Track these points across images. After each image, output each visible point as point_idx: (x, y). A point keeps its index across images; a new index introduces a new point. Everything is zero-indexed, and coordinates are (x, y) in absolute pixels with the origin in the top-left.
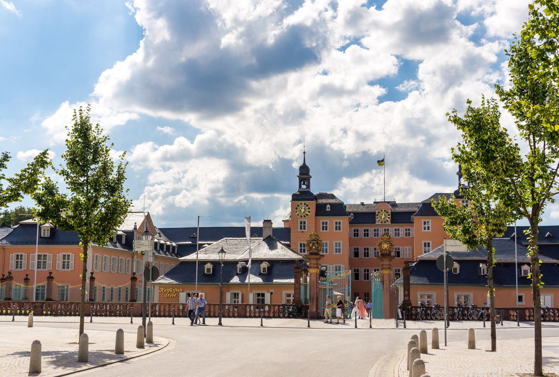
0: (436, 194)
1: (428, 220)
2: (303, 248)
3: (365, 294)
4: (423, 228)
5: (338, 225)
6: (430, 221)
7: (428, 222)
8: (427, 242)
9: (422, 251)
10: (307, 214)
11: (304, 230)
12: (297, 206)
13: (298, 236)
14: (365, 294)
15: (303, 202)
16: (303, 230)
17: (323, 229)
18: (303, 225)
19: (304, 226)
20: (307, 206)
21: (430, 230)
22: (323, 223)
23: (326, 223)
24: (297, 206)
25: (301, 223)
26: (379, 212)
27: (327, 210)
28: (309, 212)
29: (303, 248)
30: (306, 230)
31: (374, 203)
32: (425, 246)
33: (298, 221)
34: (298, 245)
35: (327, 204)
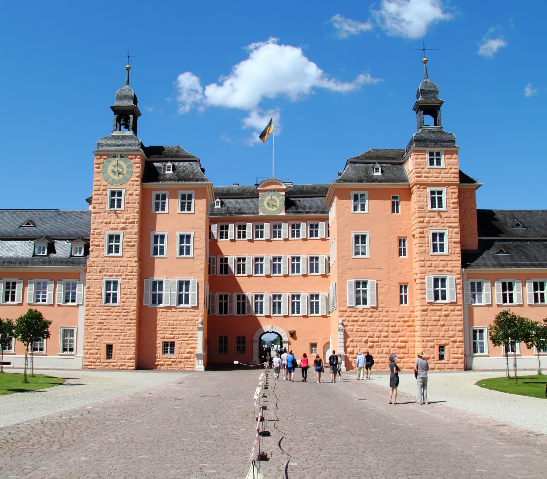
0: (373, 150)
3: (238, 338)
9: (350, 251)
12: (107, 162)
13: (105, 221)
14: (238, 338)
16: (116, 208)
18: (116, 197)
19: (119, 201)
22: (158, 197)
25: (113, 194)
27: (167, 172)
29: (114, 244)
30: (122, 208)
31: (255, 185)
32: (357, 242)
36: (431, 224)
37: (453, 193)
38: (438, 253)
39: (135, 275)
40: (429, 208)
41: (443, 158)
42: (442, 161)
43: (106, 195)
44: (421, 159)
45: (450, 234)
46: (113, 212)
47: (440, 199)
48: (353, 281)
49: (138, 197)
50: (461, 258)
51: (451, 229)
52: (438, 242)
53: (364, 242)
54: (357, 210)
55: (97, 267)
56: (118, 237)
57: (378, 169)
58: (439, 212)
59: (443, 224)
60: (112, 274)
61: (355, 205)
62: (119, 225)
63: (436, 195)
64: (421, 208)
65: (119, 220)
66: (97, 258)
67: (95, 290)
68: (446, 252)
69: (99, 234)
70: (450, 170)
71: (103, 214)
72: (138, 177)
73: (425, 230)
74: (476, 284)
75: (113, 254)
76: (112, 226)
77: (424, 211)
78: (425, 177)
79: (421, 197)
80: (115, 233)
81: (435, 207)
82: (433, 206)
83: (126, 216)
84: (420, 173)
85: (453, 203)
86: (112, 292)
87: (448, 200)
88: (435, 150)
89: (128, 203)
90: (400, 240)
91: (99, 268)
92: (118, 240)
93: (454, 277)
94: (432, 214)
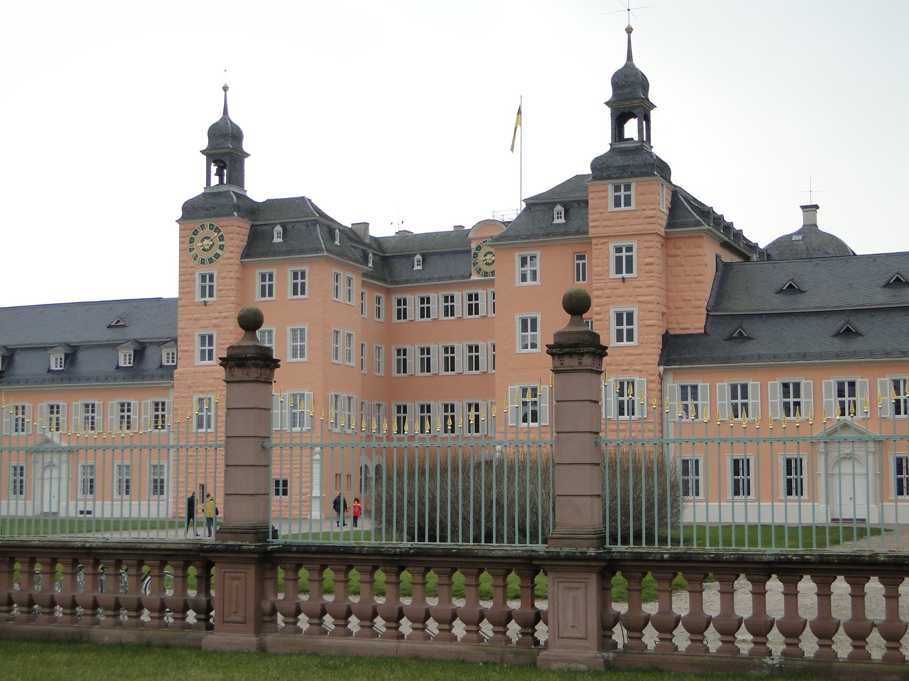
1: (532, 253)
2: (207, 348)
4: (518, 277)
6: (538, 253)
7: (533, 258)
8: (529, 315)
11: (211, 299)
13: (195, 316)
15: (207, 223)
20: (217, 230)
24: (194, 234)
25: (203, 278)
26: (479, 248)
28: (221, 247)
32: (524, 329)
33: (194, 274)
35: (275, 225)
36: (613, 299)
38: (625, 343)
41: (633, 193)
43: (194, 280)
44: (600, 198)
45: (642, 313)
46: (203, 303)
47: (629, 259)
48: (517, 387)
51: (643, 306)
52: (625, 327)
53: (534, 329)
54: (526, 281)
55: (186, 380)
57: (561, 213)
58: (623, 279)
59: (632, 299)
60: (203, 389)
61: (523, 273)
63: (624, 254)
65: (211, 315)
66: (185, 369)
69: (187, 335)
70: (644, 212)
71: (191, 308)
73: (605, 308)
74: (689, 389)
76: (203, 323)
77: (603, 279)
78: (604, 226)
79: (598, 258)
81: (621, 273)
82: (619, 270)
83: (220, 308)
84: (597, 221)
85: (647, 264)
87: (640, 260)
88: (622, 182)
89: (220, 290)
91: (189, 382)
94: (616, 284)
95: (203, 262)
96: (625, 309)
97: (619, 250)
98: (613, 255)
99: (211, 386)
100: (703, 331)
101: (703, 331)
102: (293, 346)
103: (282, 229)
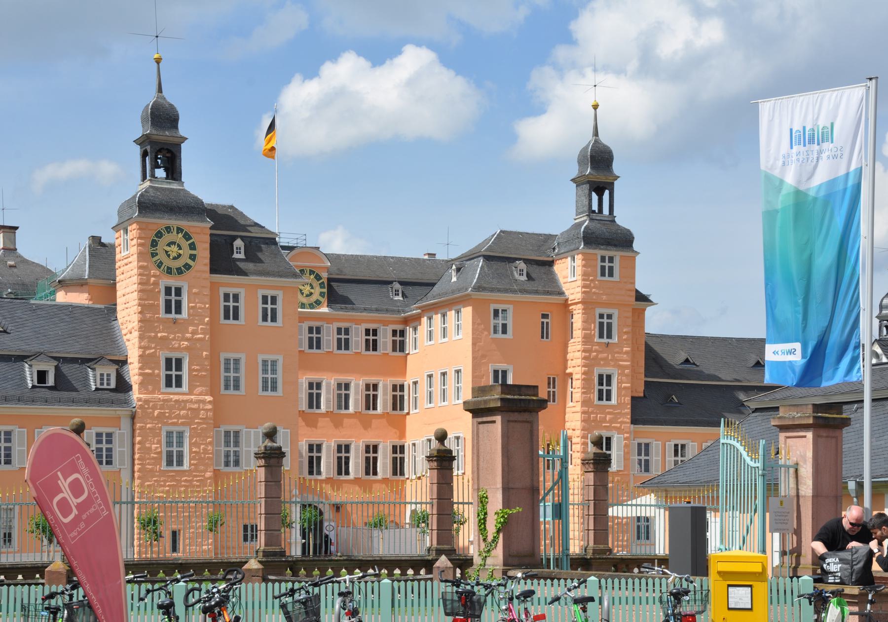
2: (174, 373)
5: (231, 304)
10: (187, 264)
11: (178, 316)
17: (227, 317)
18: (173, 298)
19: (179, 305)
21: (510, 334)
22: (227, 297)
23: (236, 298)
25: (168, 290)
29: (174, 373)
30: (185, 314)
34: (159, 363)
35: (234, 238)
37: (627, 317)
39: (210, 423)
40: (597, 339)
42: (616, 271)
43: (159, 292)
47: (609, 325)
49: (207, 299)
50: (632, 410)
56: (179, 362)
62: (182, 343)
64: (587, 339)
67: (151, 447)
68: (614, 401)
72: (205, 265)
74: (643, 445)
75: (174, 389)
80: (174, 355)
82: (601, 336)
86: (175, 449)
88: (607, 253)
90: (549, 378)
92: (179, 367)
93: (622, 436)
95: (169, 271)
96: (605, 371)
97: (601, 316)
98: (598, 320)
99: (183, 417)
100: (642, 395)
101: (642, 395)
102: (263, 378)
103: (243, 244)
